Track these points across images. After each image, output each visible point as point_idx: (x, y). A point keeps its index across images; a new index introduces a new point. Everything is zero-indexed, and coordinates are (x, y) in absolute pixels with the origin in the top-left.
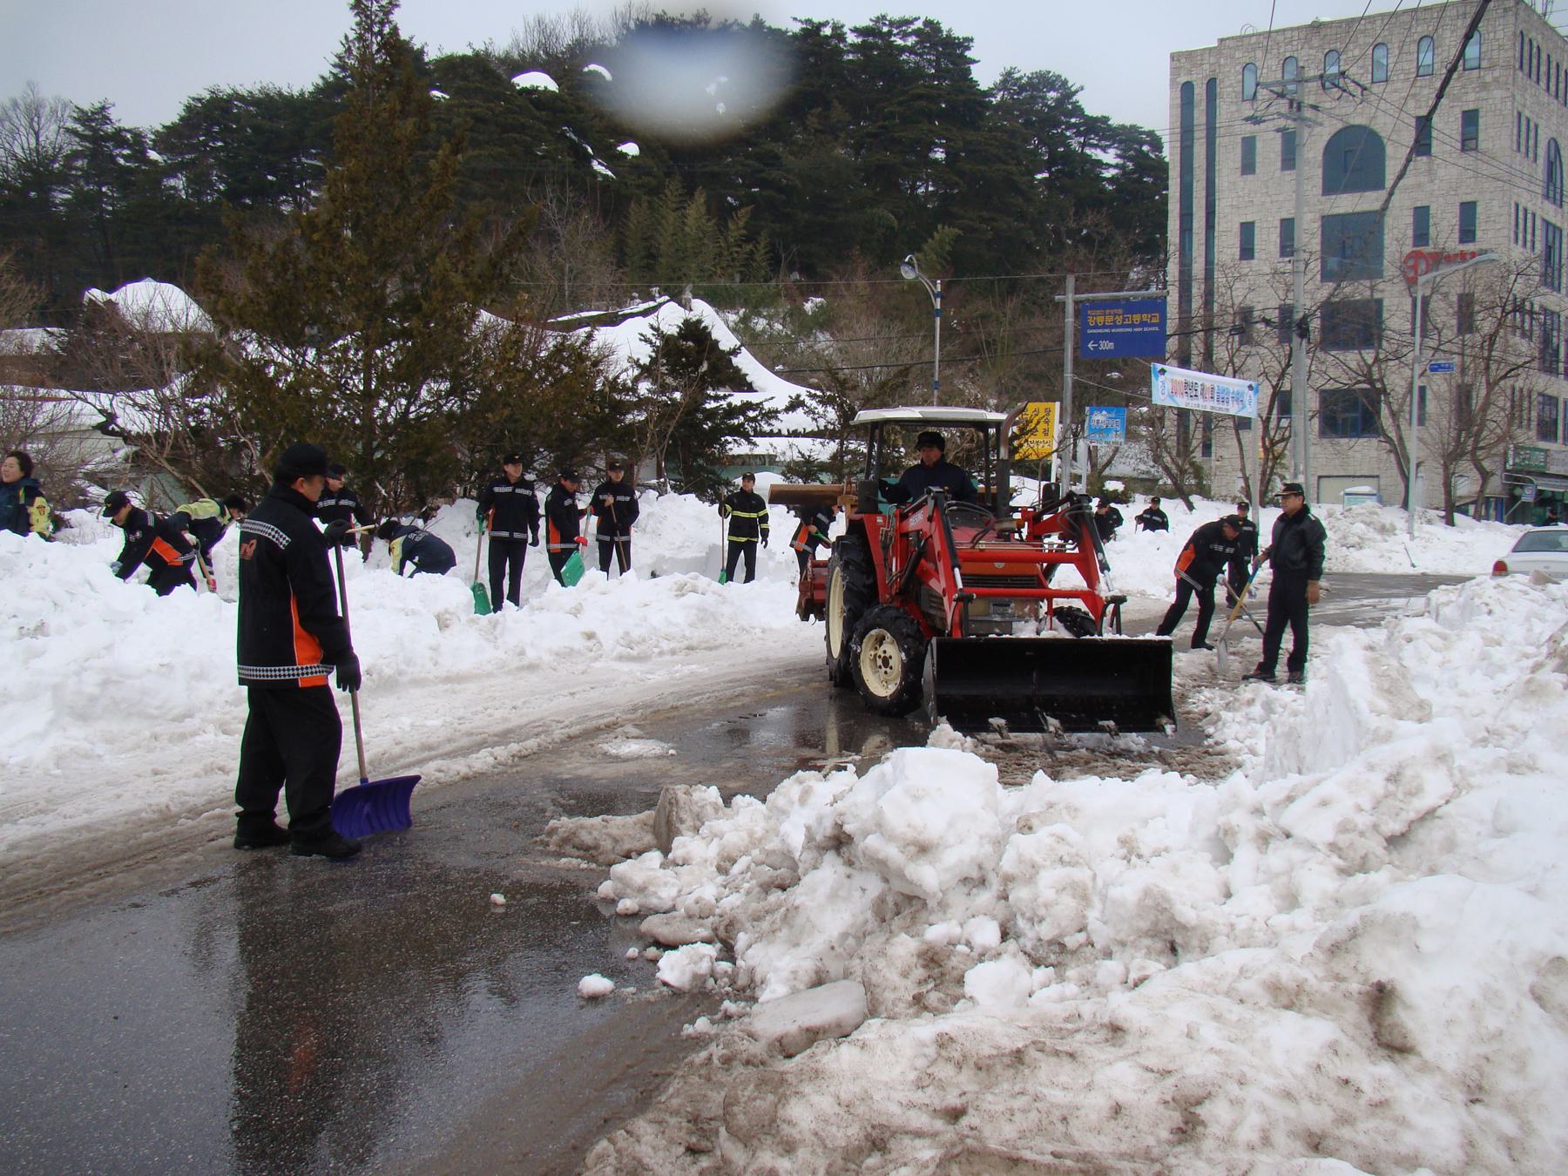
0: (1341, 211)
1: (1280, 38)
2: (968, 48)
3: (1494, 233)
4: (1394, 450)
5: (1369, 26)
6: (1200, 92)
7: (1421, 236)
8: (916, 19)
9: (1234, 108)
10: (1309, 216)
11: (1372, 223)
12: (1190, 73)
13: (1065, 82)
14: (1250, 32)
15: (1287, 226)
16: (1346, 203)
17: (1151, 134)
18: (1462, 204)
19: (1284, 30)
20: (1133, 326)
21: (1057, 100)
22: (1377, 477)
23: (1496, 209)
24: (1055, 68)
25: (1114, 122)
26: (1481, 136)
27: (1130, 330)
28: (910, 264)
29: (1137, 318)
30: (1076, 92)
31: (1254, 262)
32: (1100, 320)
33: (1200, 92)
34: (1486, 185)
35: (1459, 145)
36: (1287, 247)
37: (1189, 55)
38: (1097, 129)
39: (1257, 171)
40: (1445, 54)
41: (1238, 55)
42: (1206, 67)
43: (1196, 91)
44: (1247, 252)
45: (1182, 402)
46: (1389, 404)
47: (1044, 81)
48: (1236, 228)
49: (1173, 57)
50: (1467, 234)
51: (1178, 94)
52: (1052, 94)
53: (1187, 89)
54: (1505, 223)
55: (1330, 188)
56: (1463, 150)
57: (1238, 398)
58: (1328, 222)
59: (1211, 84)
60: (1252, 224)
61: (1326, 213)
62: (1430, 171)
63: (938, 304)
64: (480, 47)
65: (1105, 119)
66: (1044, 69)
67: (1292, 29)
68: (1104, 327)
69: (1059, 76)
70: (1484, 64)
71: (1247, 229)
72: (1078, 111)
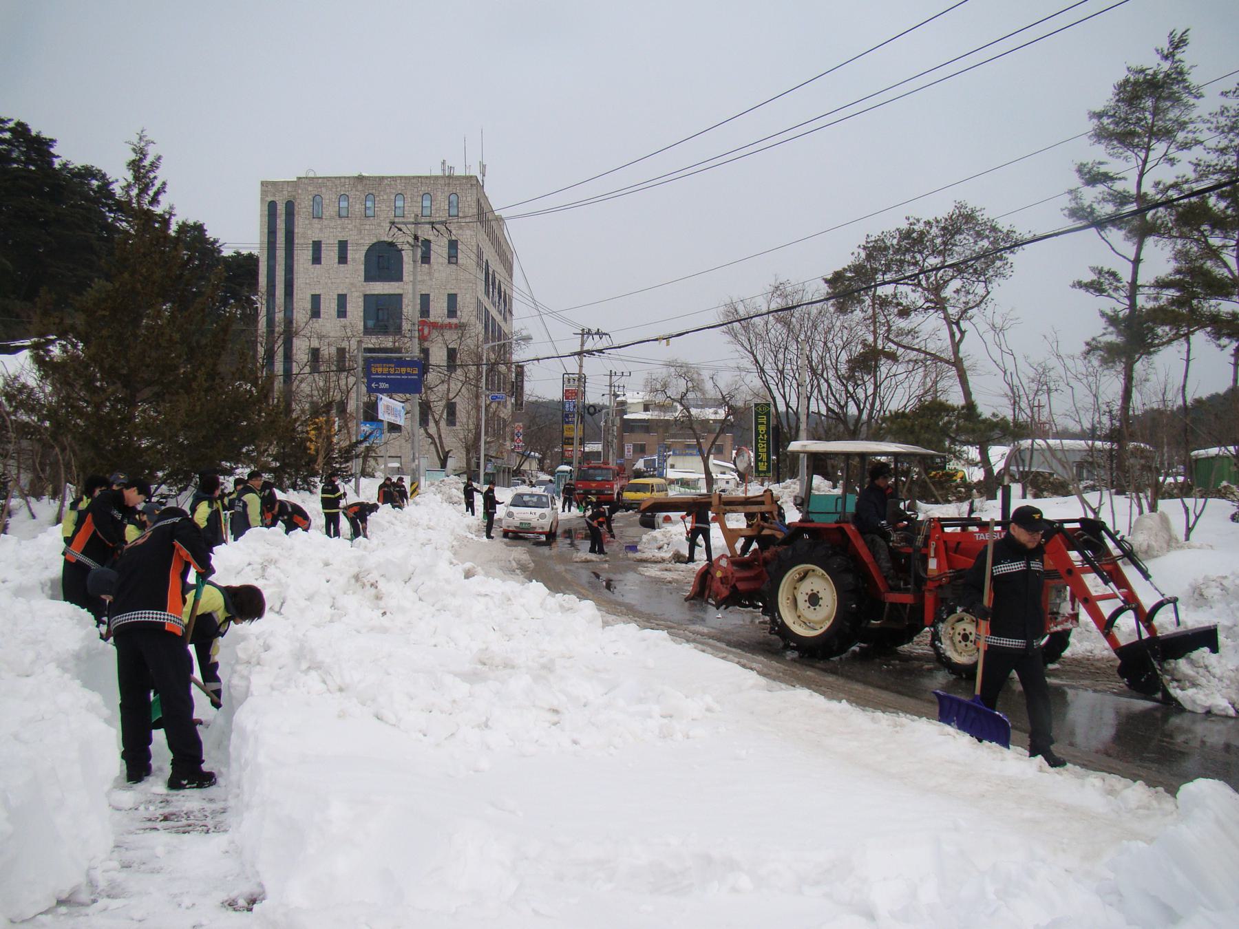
0: (376, 292)
1: (338, 182)
2: (52, 146)
3: (466, 313)
4: (434, 443)
5: (393, 183)
7: (425, 311)
9: (307, 222)
10: (356, 294)
12: (274, 195)
13: (104, 176)
14: (311, 175)
15: (342, 299)
16: (380, 288)
18: (448, 294)
19: (340, 178)
20: (401, 374)
22: (400, 457)
23: (468, 300)
24: (98, 164)
26: (460, 256)
27: (399, 377)
29: (403, 370)
30: (113, 182)
31: (320, 320)
32: (380, 370)
34: (463, 285)
35: (447, 261)
36: (342, 313)
37: (274, 184)
39: (322, 263)
40: (438, 205)
41: (310, 188)
42: (285, 193)
43: (279, 207)
44: (316, 313)
46: (433, 416)
48: (309, 298)
49: (263, 183)
50: (452, 312)
51: (266, 208)
52: (95, 183)
53: (272, 207)
54: (473, 307)
55: (368, 278)
56: (449, 262)
58: (367, 298)
60: (319, 295)
61: (368, 293)
62: (429, 273)
66: (89, 164)
67: (345, 177)
68: (382, 374)
69: (100, 171)
70: (460, 215)
71: (316, 299)
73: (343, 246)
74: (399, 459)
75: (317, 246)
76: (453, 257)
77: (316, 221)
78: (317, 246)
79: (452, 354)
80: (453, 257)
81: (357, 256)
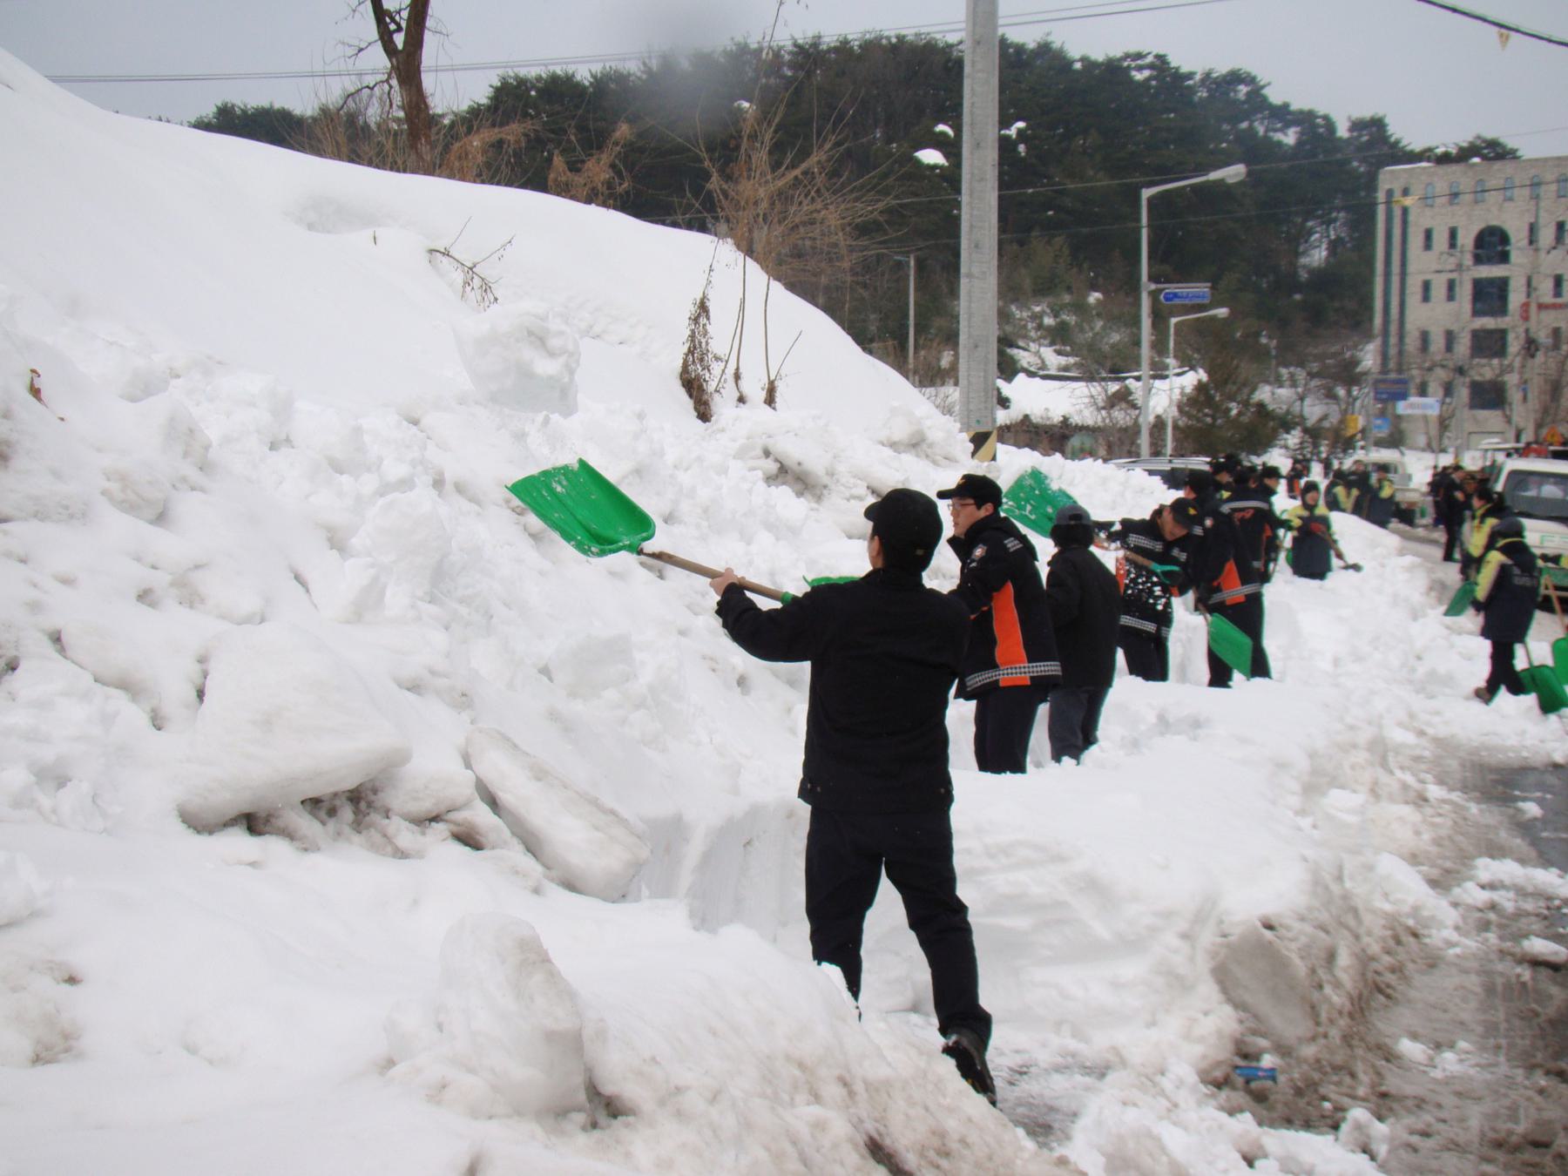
8: (1149, 53)
11: (1502, 285)
17: (1326, 118)
21: (1248, 94)
22: (1502, 433)
25: (1294, 107)
28: (1265, 336)
38: (1283, 115)
41: (1423, 178)
45: (1409, 412)
47: (1235, 78)
55: (1478, 260)
57: (1431, 407)
63: (1274, 352)
64: (739, 39)
65: (1286, 106)
66: (1237, 67)
72: (1264, 99)
73: (1453, 234)
74: (1500, 435)
75: (1428, 235)
77: (1427, 209)
78: (1428, 235)
81: (1467, 239)
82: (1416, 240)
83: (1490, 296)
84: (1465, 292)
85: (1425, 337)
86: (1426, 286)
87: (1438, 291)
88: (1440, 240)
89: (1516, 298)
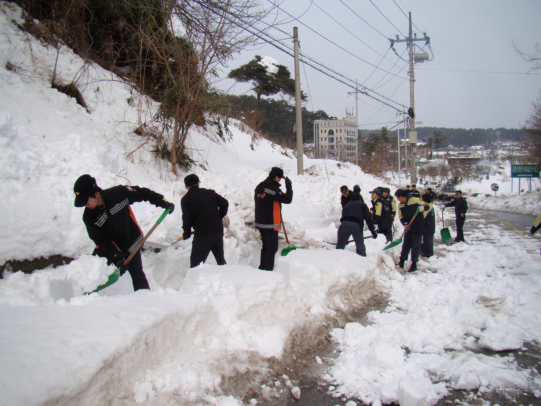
6: (317, 125)
7: (337, 140)
16: (331, 136)
33: (317, 125)
50: (341, 140)
59: (318, 124)
73: (325, 130)
75: (322, 131)
76: (341, 131)
78: (322, 131)
79: (341, 145)
80: (341, 131)
81: (327, 132)
82: (320, 132)
83: (332, 140)
84: (327, 139)
85: (322, 146)
86: (322, 138)
87: (324, 139)
88: (324, 131)
89: (335, 140)
